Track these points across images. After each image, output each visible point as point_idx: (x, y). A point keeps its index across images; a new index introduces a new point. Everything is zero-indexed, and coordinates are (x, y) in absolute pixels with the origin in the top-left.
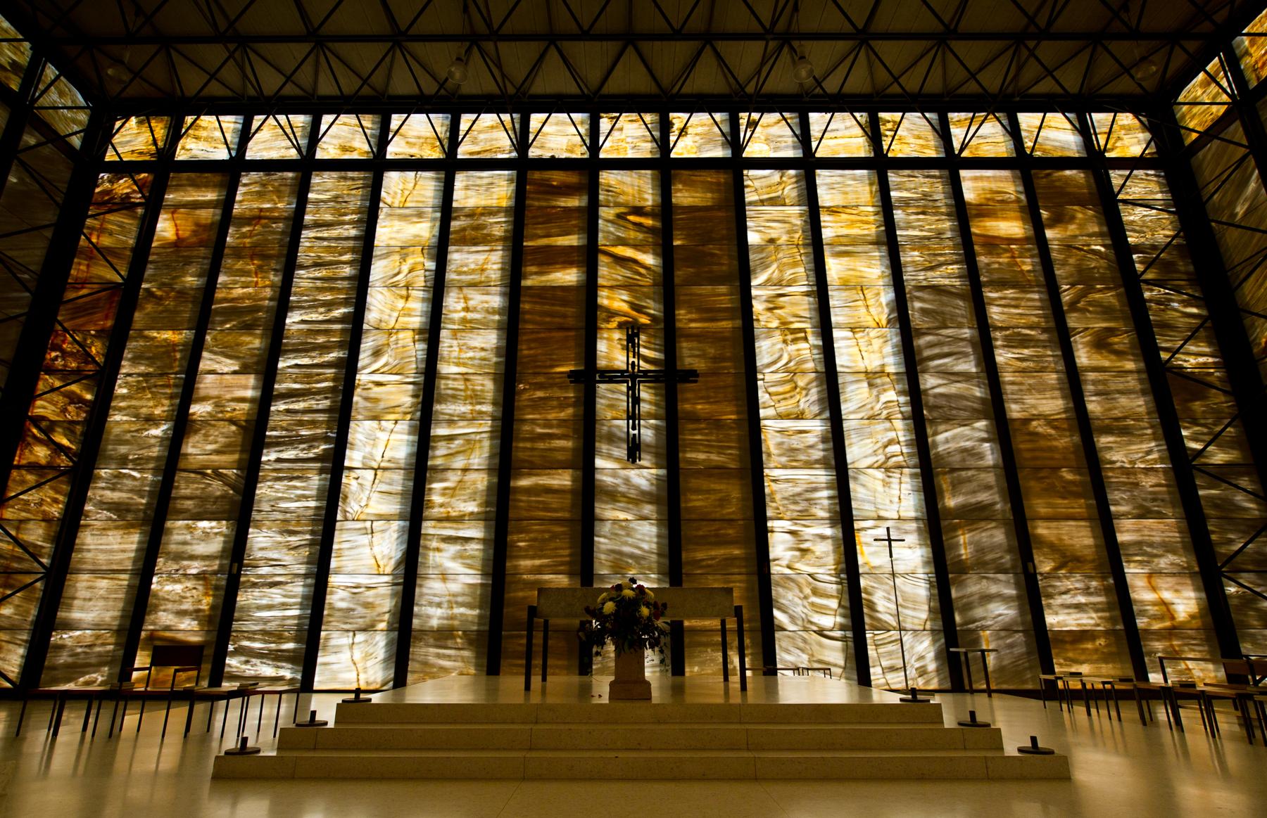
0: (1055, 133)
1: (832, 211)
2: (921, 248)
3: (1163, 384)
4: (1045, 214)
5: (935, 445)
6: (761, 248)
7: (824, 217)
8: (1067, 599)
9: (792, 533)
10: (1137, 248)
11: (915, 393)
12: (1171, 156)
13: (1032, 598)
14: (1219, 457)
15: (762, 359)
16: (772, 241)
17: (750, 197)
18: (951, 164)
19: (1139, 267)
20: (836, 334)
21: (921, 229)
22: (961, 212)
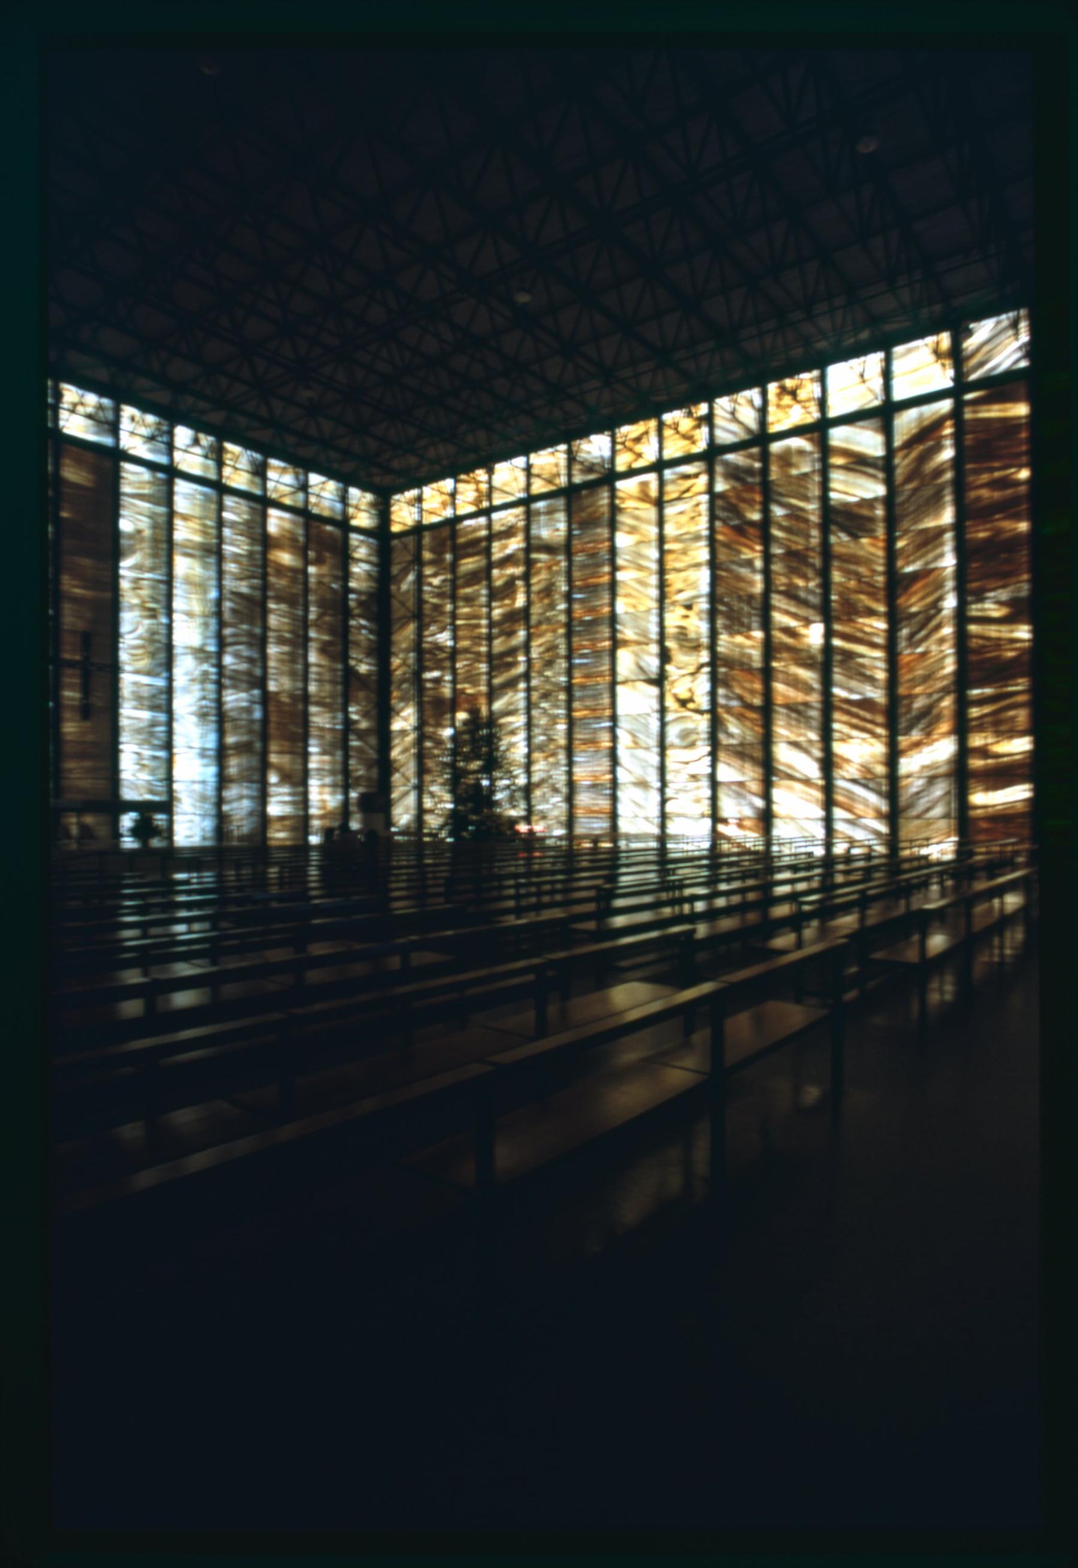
0: (324, 491)
1: (185, 518)
2: (235, 562)
3: (348, 680)
4: (311, 554)
5: (225, 703)
6: (131, 536)
7: (178, 522)
8: (279, 798)
9: (138, 754)
10: (353, 591)
11: (220, 666)
12: (381, 533)
13: (263, 798)
14: (364, 725)
15: (124, 628)
16: (139, 532)
17: (126, 489)
18: (262, 503)
19: (352, 604)
20: (175, 616)
21: (238, 546)
22: (265, 542)
